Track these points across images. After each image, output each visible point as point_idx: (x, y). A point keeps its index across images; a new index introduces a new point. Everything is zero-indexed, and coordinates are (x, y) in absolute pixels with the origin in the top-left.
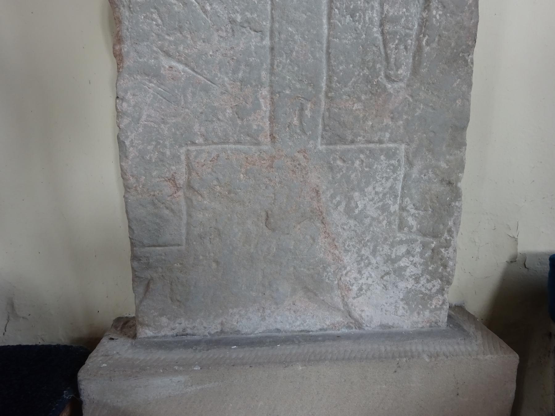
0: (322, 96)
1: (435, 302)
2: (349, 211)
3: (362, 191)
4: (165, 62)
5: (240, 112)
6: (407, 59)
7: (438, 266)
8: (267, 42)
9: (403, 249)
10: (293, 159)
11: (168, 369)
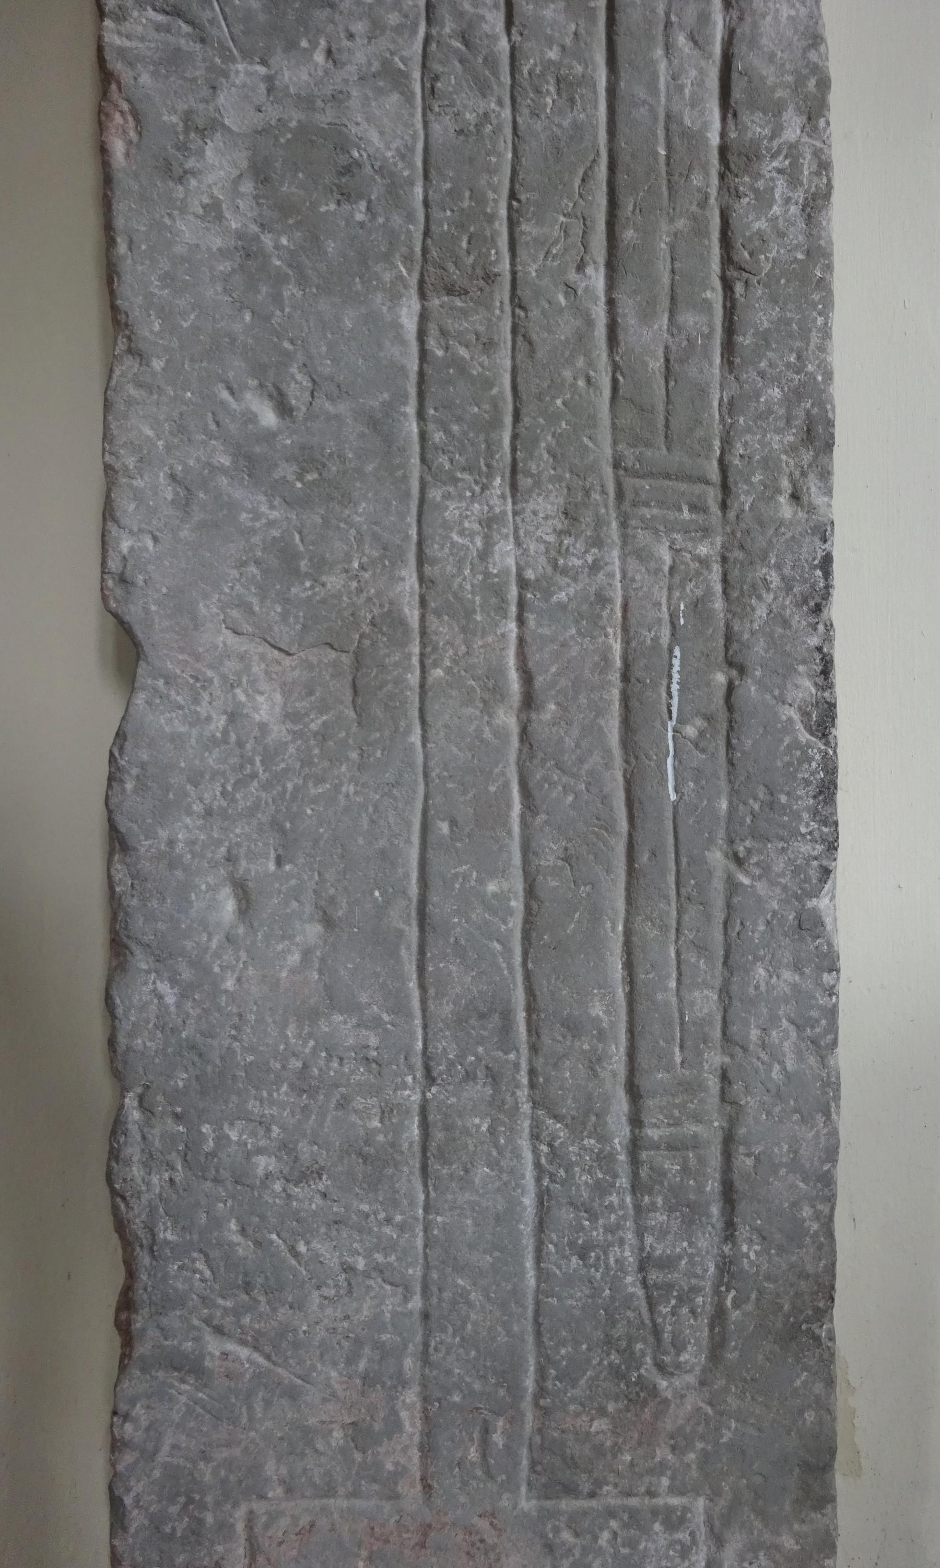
0: (527, 1405)
4: (214, 1345)
5: (361, 1436)
6: (697, 1331)
8: (416, 1303)
10: (469, 1530)
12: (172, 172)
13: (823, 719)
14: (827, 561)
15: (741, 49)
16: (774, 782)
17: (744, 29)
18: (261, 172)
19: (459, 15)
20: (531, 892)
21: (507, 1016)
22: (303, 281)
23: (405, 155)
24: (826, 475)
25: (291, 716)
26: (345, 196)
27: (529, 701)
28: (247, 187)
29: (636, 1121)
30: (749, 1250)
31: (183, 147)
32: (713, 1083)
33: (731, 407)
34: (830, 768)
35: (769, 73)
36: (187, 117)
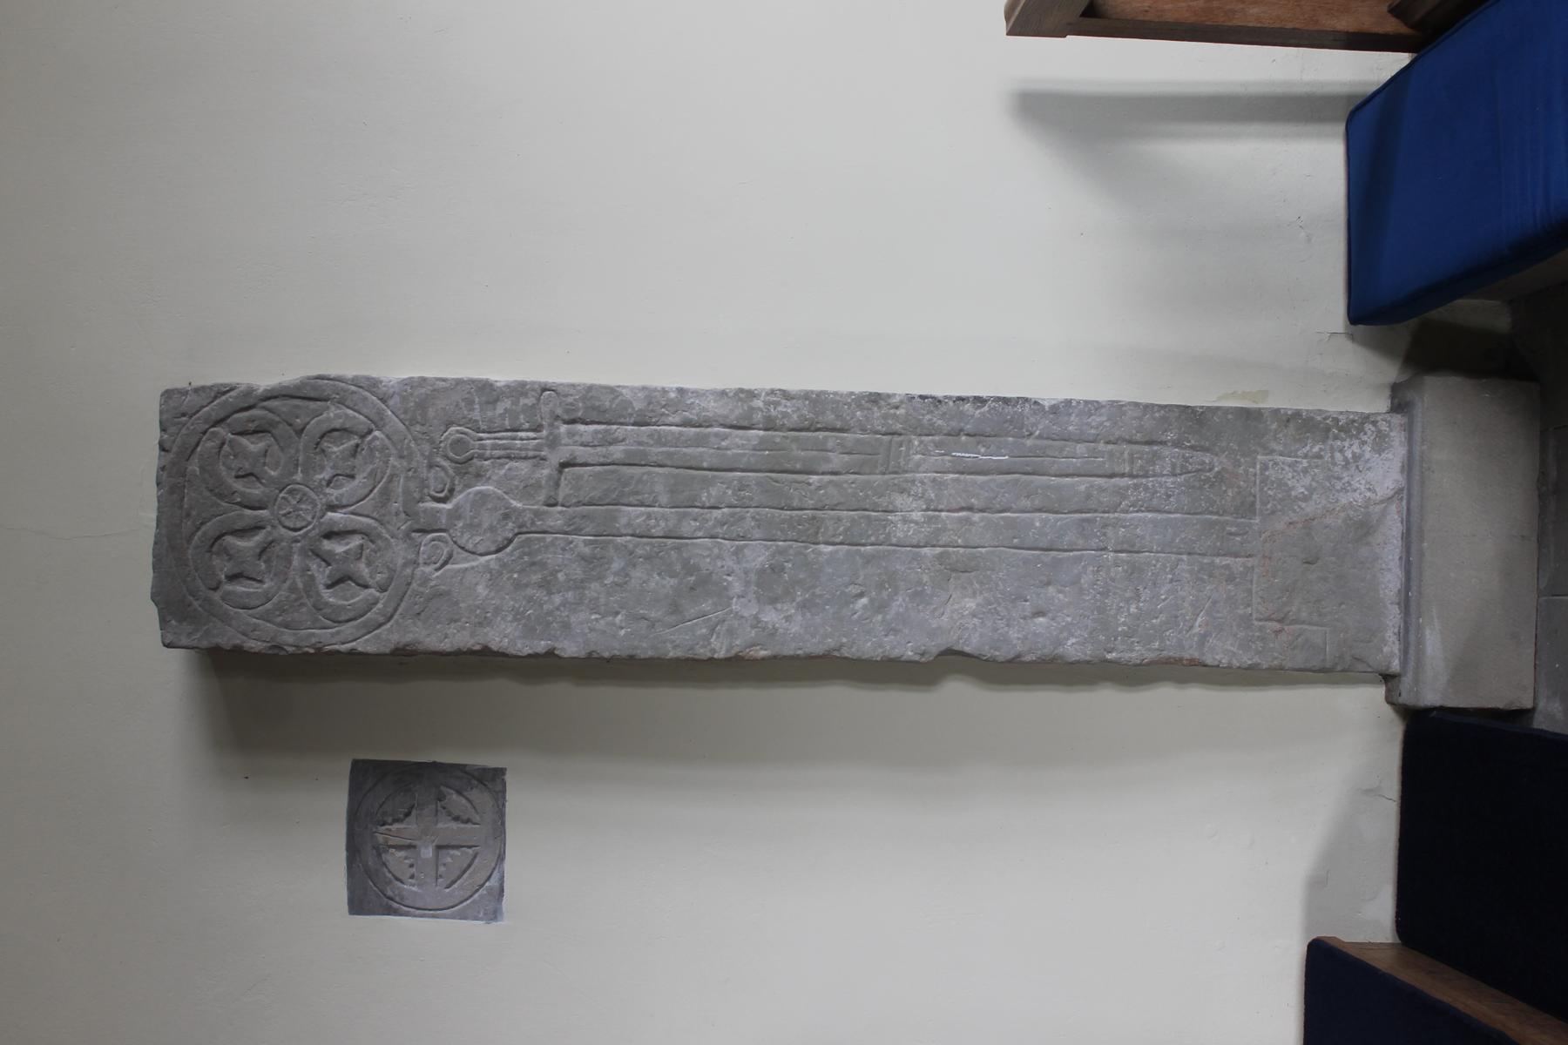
1: (1384, 427)
2: (1306, 499)
3: (1293, 488)
4: (1196, 630)
5: (1230, 579)
7: (1353, 426)
8: (1185, 557)
9: (1338, 455)
10: (1265, 541)
11: (1420, 642)
12: (774, 632)
13: (979, 401)
14: (921, 397)
15: (728, 422)
16: (1000, 420)
17: (721, 420)
18: (774, 601)
19: (714, 526)
20: (1040, 510)
21: (1084, 520)
22: (814, 587)
23: (767, 548)
24: (889, 396)
25: (974, 595)
26: (783, 569)
27: (970, 509)
28: (779, 606)
29: (1123, 475)
30: (1170, 436)
31: (764, 629)
32: (1110, 447)
33: (864, 430)
34: (998, 399)
35: (737, 412)
36: (753, 627)
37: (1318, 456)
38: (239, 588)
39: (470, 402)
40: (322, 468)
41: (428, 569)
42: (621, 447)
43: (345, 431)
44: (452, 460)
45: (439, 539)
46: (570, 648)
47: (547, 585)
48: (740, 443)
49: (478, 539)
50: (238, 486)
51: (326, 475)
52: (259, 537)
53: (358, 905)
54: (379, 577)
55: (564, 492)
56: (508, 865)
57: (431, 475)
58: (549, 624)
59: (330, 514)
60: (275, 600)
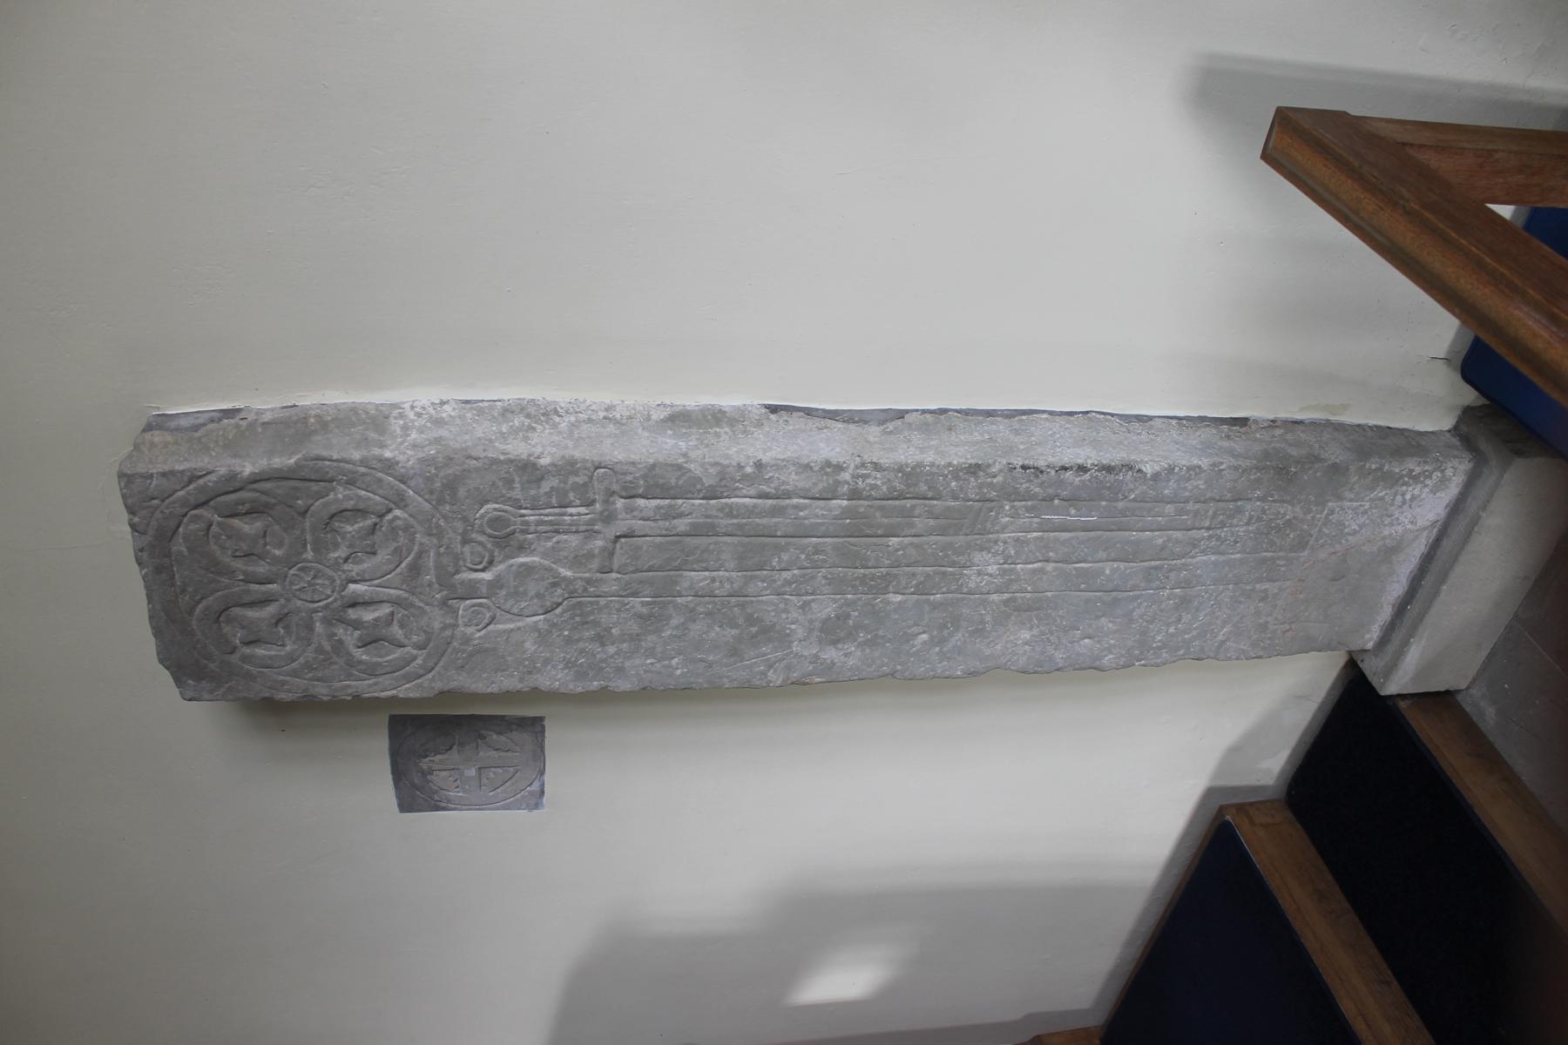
13: (1082, 469)
18: (835, 643)
23: (835, 601)
32: (1198, 506)
33: (956, 498)
35: (820, 486)
37: (1382, 499)
38: (260, 651)
39: (509, 483)
40: (336, 546)
41: (469, 630)
42: (688, 520)
43: (359, 512)
44: (490, 536)
45: (480, 605)
46: (624, 685)
47: (601, 639)
48: (818, 513)
49: (523, 604)
50: (239, 564)
51: (341, 553)
52: (271, 610)
53: (406, 806)
54: (415, 638)
55: (616, 562)
56: (546, 778)
57: (467, 549)
58: (602, 669)
59: (352, 586)
60: (302, 660)
